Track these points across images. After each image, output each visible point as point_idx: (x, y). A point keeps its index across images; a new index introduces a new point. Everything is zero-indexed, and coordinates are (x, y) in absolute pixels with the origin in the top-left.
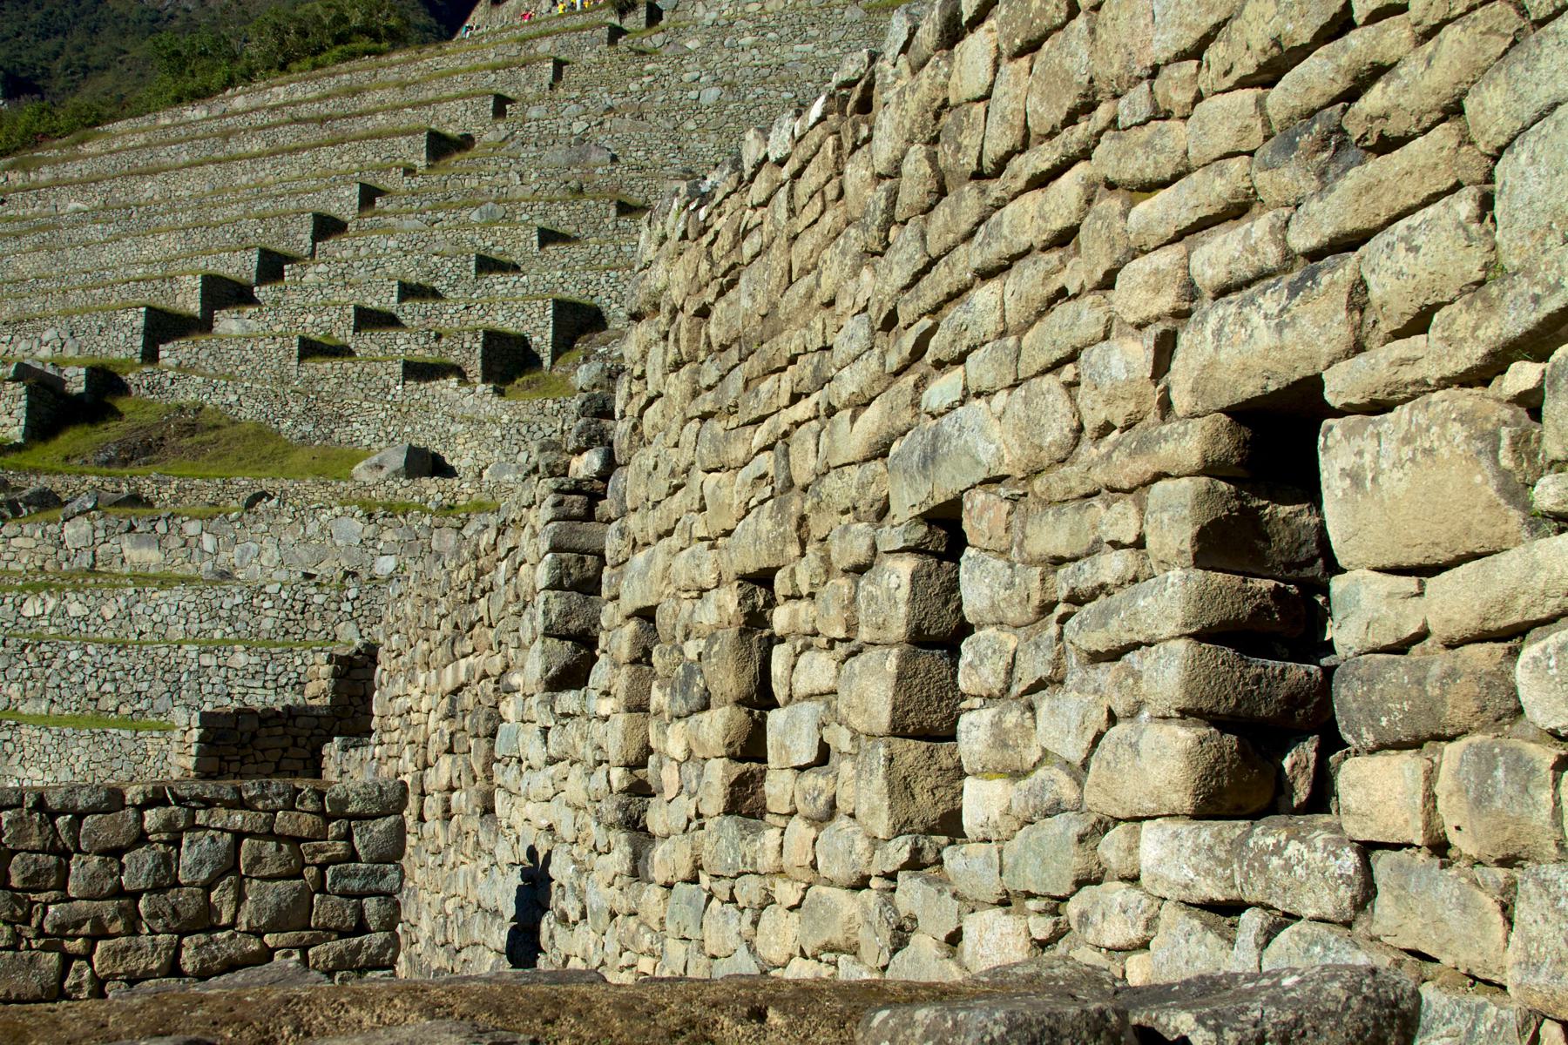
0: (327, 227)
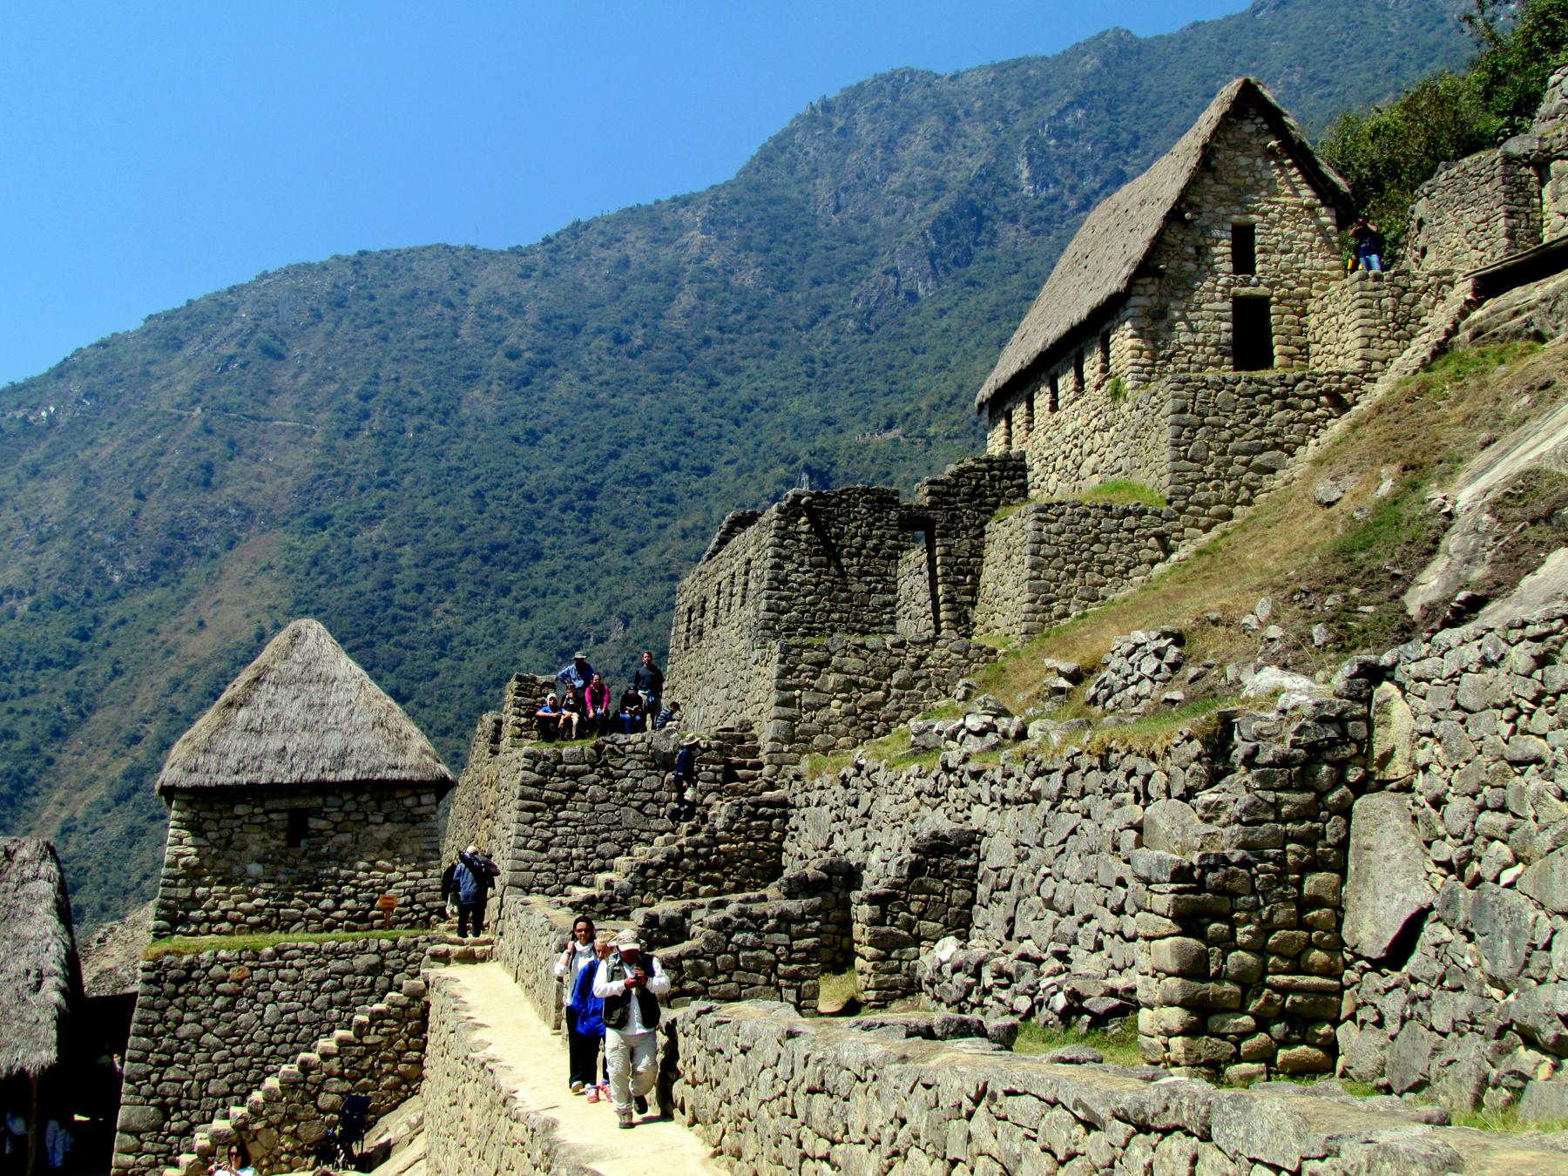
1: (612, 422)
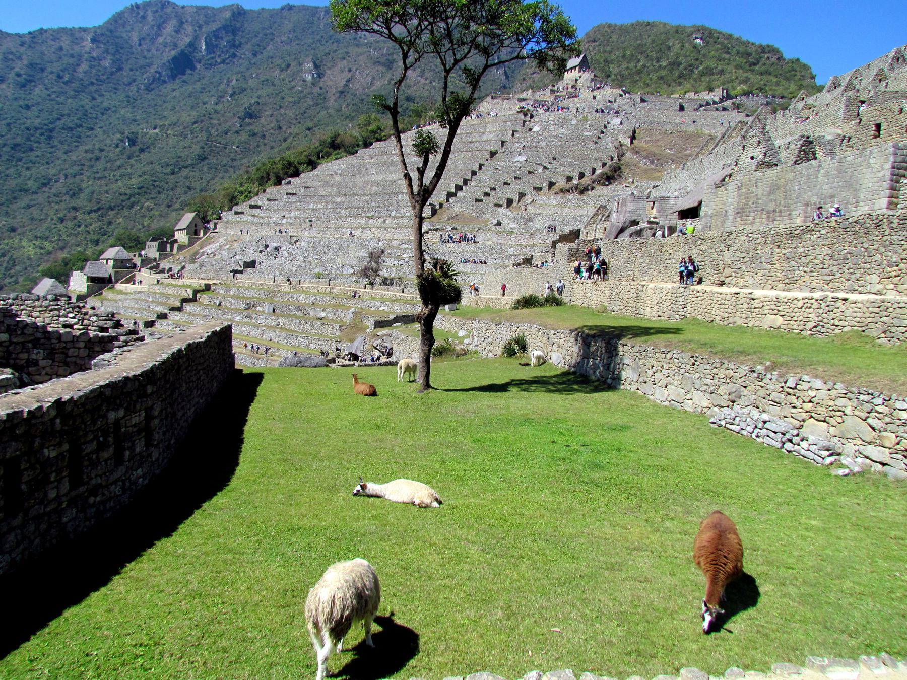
0: (474, 173)
1: (57, 107)
